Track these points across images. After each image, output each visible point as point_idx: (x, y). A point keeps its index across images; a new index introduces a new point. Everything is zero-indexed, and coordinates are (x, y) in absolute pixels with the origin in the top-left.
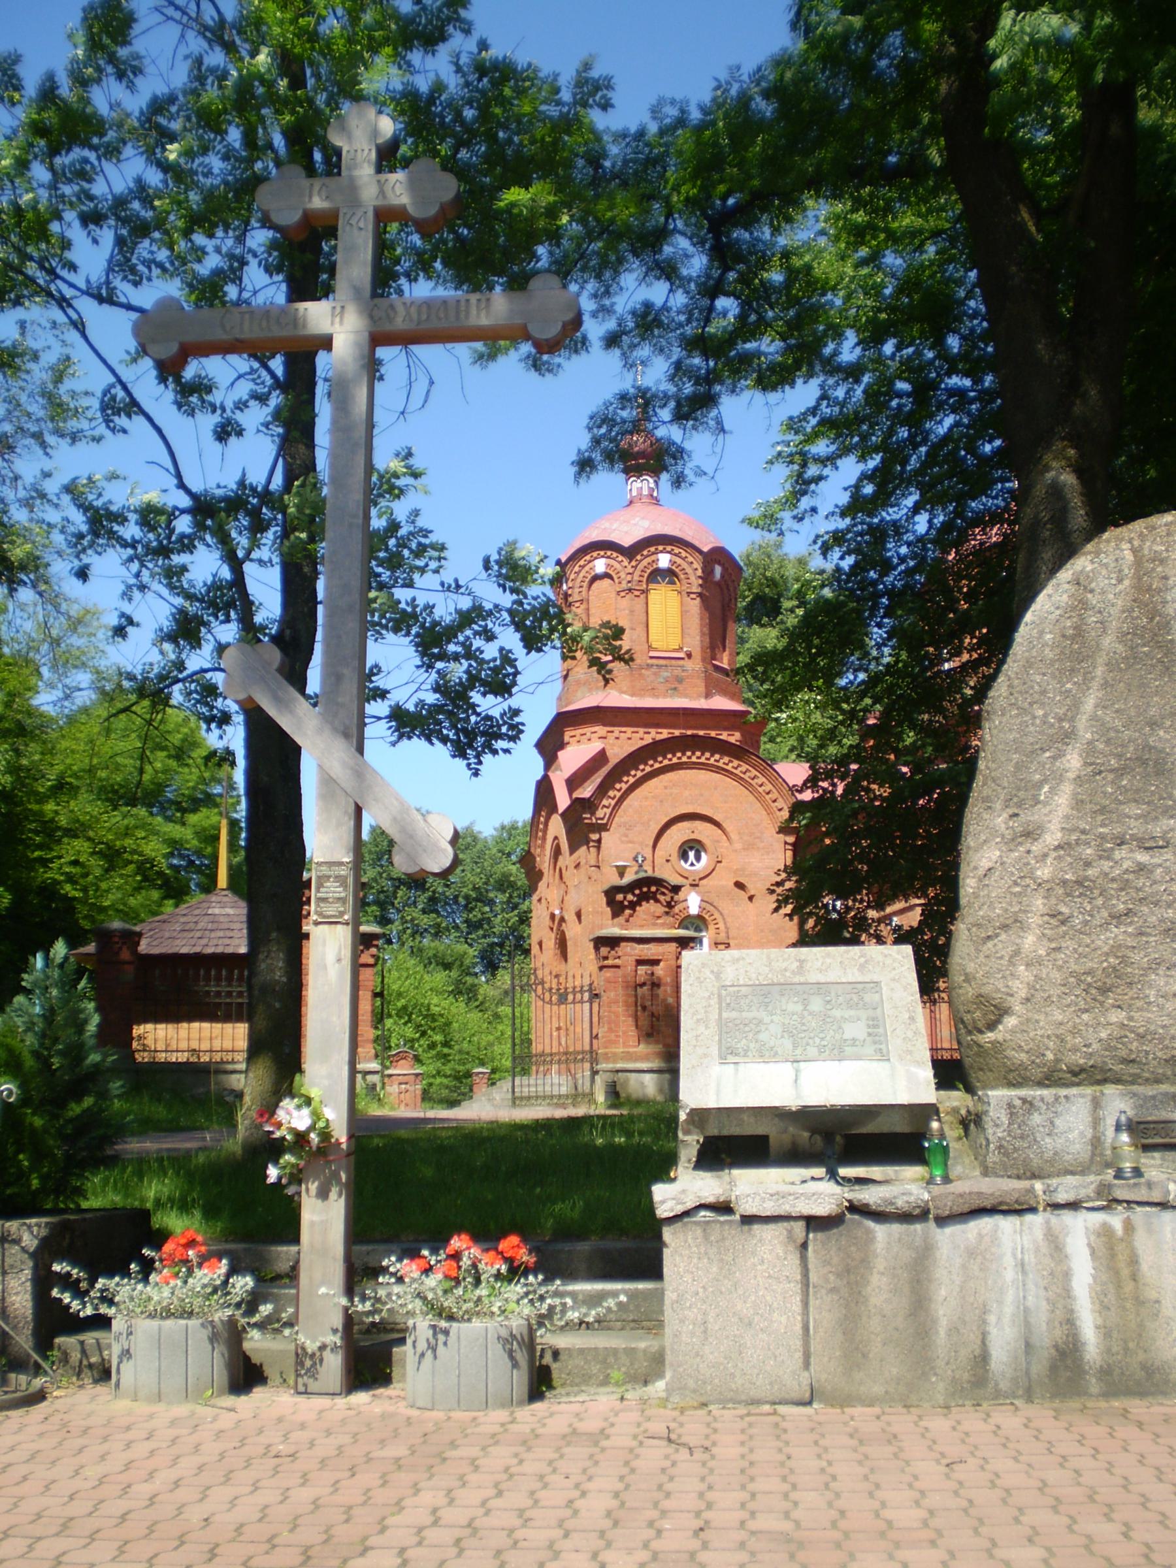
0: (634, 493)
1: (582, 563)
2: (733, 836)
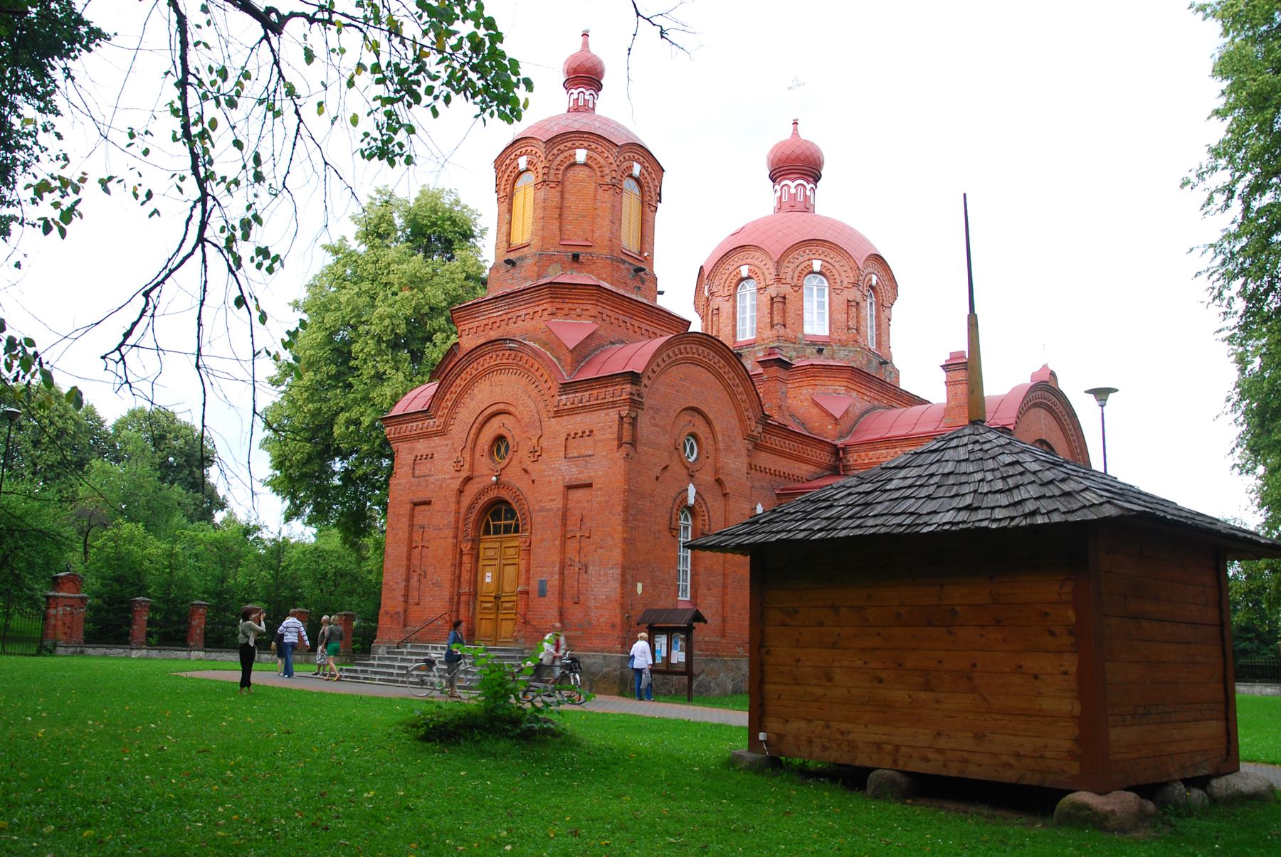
0: (581, 103)
1: (562, 147)
2: (720, 437)
